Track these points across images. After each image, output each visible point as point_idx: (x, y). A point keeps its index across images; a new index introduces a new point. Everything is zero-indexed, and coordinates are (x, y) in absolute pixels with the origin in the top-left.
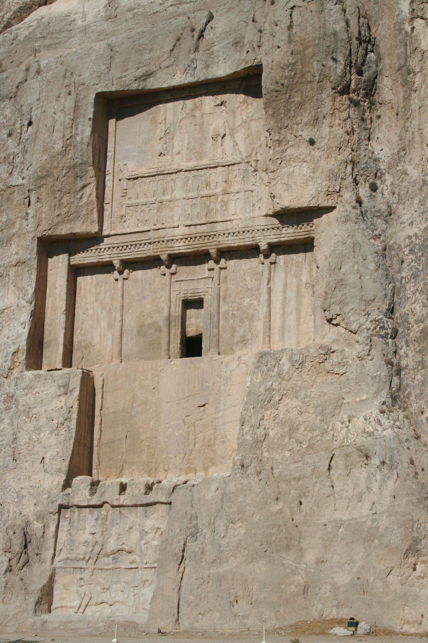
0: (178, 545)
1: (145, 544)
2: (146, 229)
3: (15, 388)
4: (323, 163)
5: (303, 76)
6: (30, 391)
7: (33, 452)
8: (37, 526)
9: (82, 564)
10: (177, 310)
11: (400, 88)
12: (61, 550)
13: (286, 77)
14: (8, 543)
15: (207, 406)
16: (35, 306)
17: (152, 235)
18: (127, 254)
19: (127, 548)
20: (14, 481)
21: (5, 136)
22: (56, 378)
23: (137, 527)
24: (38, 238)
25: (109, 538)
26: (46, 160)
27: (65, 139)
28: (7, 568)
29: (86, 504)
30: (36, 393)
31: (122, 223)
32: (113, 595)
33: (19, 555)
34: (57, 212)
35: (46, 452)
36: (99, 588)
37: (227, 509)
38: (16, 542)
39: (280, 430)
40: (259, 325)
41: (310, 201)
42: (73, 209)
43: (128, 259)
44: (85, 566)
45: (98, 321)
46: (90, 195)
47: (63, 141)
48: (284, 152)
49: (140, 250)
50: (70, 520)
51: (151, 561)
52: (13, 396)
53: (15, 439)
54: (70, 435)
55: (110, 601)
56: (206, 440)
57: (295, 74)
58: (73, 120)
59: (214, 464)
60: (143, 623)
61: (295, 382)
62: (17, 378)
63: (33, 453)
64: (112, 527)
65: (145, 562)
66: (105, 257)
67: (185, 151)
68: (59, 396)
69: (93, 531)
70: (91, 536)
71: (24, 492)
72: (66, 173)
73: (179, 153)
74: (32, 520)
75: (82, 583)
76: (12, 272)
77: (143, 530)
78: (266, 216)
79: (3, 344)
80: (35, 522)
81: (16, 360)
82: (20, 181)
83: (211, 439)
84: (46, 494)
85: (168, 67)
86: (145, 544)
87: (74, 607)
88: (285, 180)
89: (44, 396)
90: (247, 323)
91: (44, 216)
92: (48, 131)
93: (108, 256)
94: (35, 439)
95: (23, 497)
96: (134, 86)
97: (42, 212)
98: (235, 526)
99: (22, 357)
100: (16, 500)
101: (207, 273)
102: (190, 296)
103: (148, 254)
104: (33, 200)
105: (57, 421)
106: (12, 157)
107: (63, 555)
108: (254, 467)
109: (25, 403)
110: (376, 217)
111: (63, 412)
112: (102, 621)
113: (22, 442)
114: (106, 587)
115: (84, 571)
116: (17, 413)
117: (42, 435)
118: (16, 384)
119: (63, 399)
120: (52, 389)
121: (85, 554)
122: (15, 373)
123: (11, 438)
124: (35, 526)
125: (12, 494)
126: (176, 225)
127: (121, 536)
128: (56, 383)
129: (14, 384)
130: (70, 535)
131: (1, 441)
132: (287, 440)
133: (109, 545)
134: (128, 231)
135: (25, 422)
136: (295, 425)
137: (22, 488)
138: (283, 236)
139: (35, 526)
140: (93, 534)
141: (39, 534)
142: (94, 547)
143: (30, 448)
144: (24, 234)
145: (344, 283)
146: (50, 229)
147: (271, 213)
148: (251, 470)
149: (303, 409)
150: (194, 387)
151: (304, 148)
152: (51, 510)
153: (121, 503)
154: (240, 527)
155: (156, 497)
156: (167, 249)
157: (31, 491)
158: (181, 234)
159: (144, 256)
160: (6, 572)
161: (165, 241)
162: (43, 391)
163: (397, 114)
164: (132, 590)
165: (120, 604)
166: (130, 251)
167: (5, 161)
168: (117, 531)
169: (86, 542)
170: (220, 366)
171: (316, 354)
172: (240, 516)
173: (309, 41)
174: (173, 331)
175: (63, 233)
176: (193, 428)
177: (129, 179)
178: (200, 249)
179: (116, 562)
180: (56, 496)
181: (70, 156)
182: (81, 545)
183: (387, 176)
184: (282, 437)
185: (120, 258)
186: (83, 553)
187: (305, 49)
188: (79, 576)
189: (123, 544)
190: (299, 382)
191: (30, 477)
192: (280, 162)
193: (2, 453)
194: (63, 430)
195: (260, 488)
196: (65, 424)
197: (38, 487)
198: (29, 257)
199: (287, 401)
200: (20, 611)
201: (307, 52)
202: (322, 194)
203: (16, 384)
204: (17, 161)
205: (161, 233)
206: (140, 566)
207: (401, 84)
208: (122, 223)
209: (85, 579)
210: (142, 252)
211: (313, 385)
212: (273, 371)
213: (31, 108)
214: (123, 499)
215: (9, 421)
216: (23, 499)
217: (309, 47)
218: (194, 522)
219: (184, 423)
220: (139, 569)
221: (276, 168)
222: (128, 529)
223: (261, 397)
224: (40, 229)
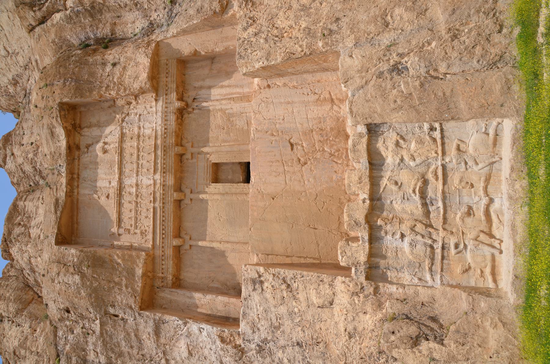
0: (411, 84)
1: (414, 160)
2: (152, 210)
3: (252, 343)
4: (129, 54)
5: (74, 73)
6: (255, 324)
7: (311, 321)
8: (389, 308)
9: (438, 247)
10: (219, 186)
11: (103, 16)
12: (420, 279)
13: (70, 83)
14: (405, 341)
15: (292, 141)
16: (190, 318)
17: (157, 205)
18: (169, 231)
19: (419, 184)
20: (338, 343)
21: (72, 336)
22: (247, 293)
23: (395, 173)
24: (141, 309)
25: (406, 212)
26: (84, 292)
27: (74, 272)
28: (438, 343)
29: (367, 245)
30: (259, 318)
31: (146, 233)
32: (477, 199)
33: (421, 326)
34: (124, 288)
35: (313, 304)
36: (469, 220)
37: (372, 35)
38: (405, 329)
39: (303, 19)
40: (236, 107)
41: (148, 57)
42: (125, 273)
43: (173, 229)
44: (440, 244)
45: (219, 267)
46: (118, 255)
47: (75, 273)
48: (115, 83)
49: (167, 217)
50: (385, 268)
51: (433, 147)
52: (258, 345)
53: (298, 344)
54: (299, 276)
55: (485, 201)
56: (322, 139)
57: (71, 78)
58: (65, 265)
59: (345, 130)
60: (515, 122)
61: (264, 20)
62: (244, 339)
63: (313, 321)
64: (393, 208)
65: (436, 155)
66: (169, 252)
67: (109, 177)
68: (263, 290)
69: (398, 236)
70: (406, 240)
71: (350, 328)
72: (97, 275)
73: (110, 182)
74: (381, 315)
75: (462, 246)
76: (162, 340)
77: (399, 164)
78: (156, 100)
79: (216, 356)
80: (384, 311)
81: (228, 340)
82: (98, 322)
83: (320, 134)
84: (354, 300)
85: (57, 189)
86: (414, 160)
87: (493, 256)
88: (132, 80)
89: (262, 308)
90: (234, 119)
91: (124, 301)
92: (68, 288)
93: (169, 250)
94: (300, 318)
95: (355, 329)
96: (58, 212)
97: (122, 303)
98: (391, 22)
99: (227, 332)
100: (358, 338)
101: (194, 160)
102: (209, 176)
103: (172, 210)
104: (112, 311)
105: (285, 292)
106: (84, 330)
107: (428, 277)
108: (331, 24)
109: (266, 331)
110: (171, 14)
111: (277, 284)
112: (513, 187)
113: (301, 334)
114: (466, 210)
115: (446, 244)
116: (274, 341)
117: (296, 310)
118: (249, 341)
119: (266, 284)
120: (256, 297)
121: (425, 244)
122: (239, 342)
123: (297, 348)
124: (390, 310)
125: (352, 344)
126: (152, 182)
127: (406, 196)
128: (251, 294)
129: (248, 344)
130: (402, 268)
131: (299, 362)
132: (312, 10)
133: (415, 211)
134: (151, 227)
135: (283, 332)
136: (300, 8)
137: (346, 330)
138: (172, 86)
139: (390, 310)
140: (403, 236)
141: (399, 306)
142: (417, 233)
143: (308, 326)
144: (136, 325)
145: (200, 8)
146: (135, 297)
147: (154, 95)
148: (334, 27)
149: (287, 6)
150: (275, 155)
151: (118, 70)
152: (371, 290)
153: (366, 196)
154: (392, 17)
155: (362, 151)
156: (170, 191)
157: (349, 320)
158: (160, 176)
159: (172, 215)
160: (442, 344)
161: (164, 192)
162: (257, 310)
163: (118, 17)
164: (470, 170)
165: (489, 186)
166: (167, 228)
167: (86, 337)
168: (399, 202)
169: (411, 244)
170: (258, 131)
171: (245, 9)
172: (379, 19)
173: (56, 71)
174: (233, 190)
175: (140, 285)
176: (310, 154)
177: (119, 227)
178: (173, 161)
179: (436, 200)
180: (357, 284)
181: (85, 269)
182: (414, 251)
183: (152, 19)
184: (309, 15)
185: (172, 238)
186: (424, 248)
187: (59, 73)
188: (453, 251)
189: (414, 191)
190: (265, 17)
191: (336, 323)
192: (120, 86)
193: (311, 361)
194: (294, 285)
195: (353, 13)
196: (289, 283)
197: (347, 311)
198: (152, 321)
199: (279, 22)
200: (499, 319)
201: (62, 72)
202: (146, 51)
203: (249, 341)
204: (87, 325)
205: (158, 195)
206: (439, 163)
207: (101, 15)
208: (146, 233)
209: (456, 240)
210: (170, 215)
211: (269, 5)
212: (252, 42)
213: (59, 308)
214: (364, 195)
215: (281, 352)
216: (358, 329)
217: (60, 71)
218: (387, 75)
219: (305, 163)
220: (444, 162)
221: (123, 88)
222: (397, 187)
223: (271, 45)
224: (133, 307)
